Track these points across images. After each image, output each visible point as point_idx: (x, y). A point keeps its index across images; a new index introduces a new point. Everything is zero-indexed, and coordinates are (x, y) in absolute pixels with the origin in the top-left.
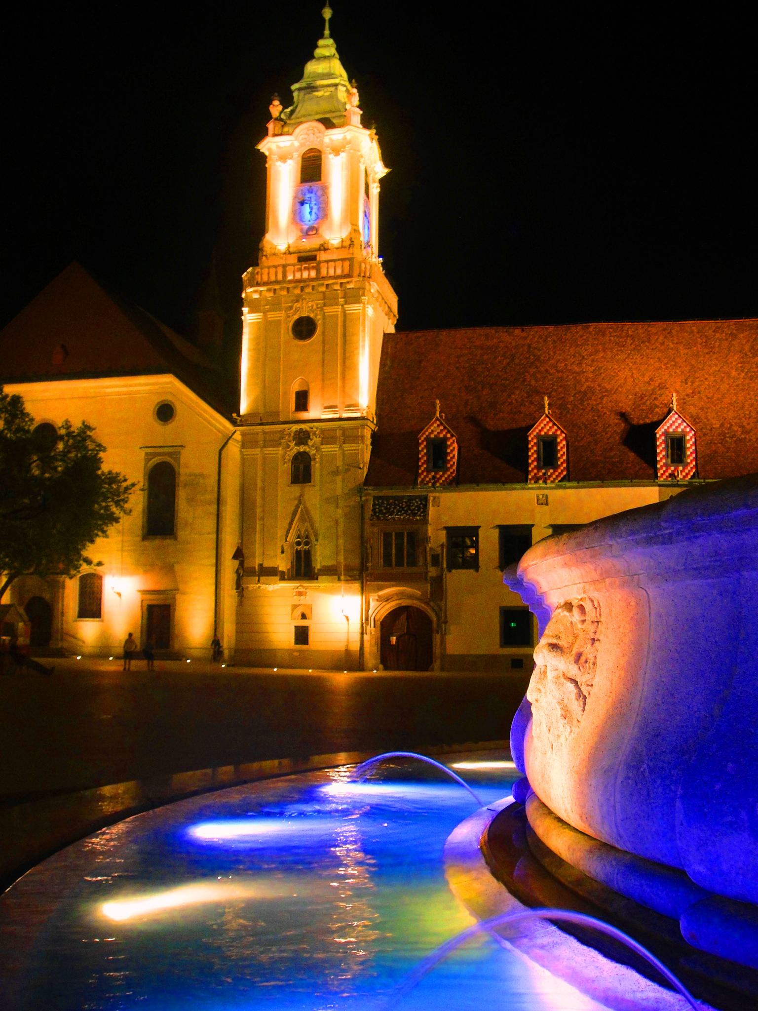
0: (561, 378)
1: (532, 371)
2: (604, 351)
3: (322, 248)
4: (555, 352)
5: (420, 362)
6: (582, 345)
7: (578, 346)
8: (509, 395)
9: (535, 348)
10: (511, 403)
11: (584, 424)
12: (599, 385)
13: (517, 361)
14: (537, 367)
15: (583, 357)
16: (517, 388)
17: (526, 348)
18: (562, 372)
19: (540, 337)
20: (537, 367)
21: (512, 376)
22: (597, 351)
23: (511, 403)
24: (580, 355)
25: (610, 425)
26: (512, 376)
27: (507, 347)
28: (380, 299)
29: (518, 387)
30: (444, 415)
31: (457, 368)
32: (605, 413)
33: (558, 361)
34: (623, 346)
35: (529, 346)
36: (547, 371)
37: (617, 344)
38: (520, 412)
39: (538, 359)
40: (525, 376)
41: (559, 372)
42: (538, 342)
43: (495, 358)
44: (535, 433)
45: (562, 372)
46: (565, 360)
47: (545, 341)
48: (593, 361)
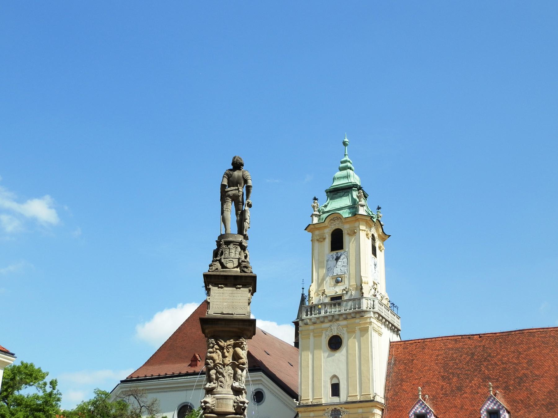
0: (505, 369)
1: (485, 364)
2: (534, 348)
3: (344, 292)
4: (501, 350)
5: (413, 360)
6: (520, 344)
7: (516, 345)
8: (470, 382)
9: (487, 348)
10: (472, 386)
11: (521, 400)
12: (531, 372)
13: (475, 357)
14: (489, 361)
15: (520, 353)
16: (476, 375)
17: (481, 348)
18: (506, 363)
19: (491, 340)
20: (489, 361)
21: (472, 368)
22: (529, 349)
23: (472, 386)
24: (518, 351)
25: (539, 400)
26: (472, 368)
27: (469, 348)
28: (384, 320)
29: (476, 375)
30: (427, 396)
31: (436, 364)
32: (535, 392)
33: (503, 356)
34: (548, 343)
35: (484, 346)
36: (496, 363)
37: (543, 342)
38: (478, 393)
39: (489, 356)
40: (481, 367)
41: (503, 363)
42: (489, 343)
43: (461, 356)
44: (485, 408)
45: (506, 363)
46: (508, 355)
47: (494, 343)
48: (527, 355)
